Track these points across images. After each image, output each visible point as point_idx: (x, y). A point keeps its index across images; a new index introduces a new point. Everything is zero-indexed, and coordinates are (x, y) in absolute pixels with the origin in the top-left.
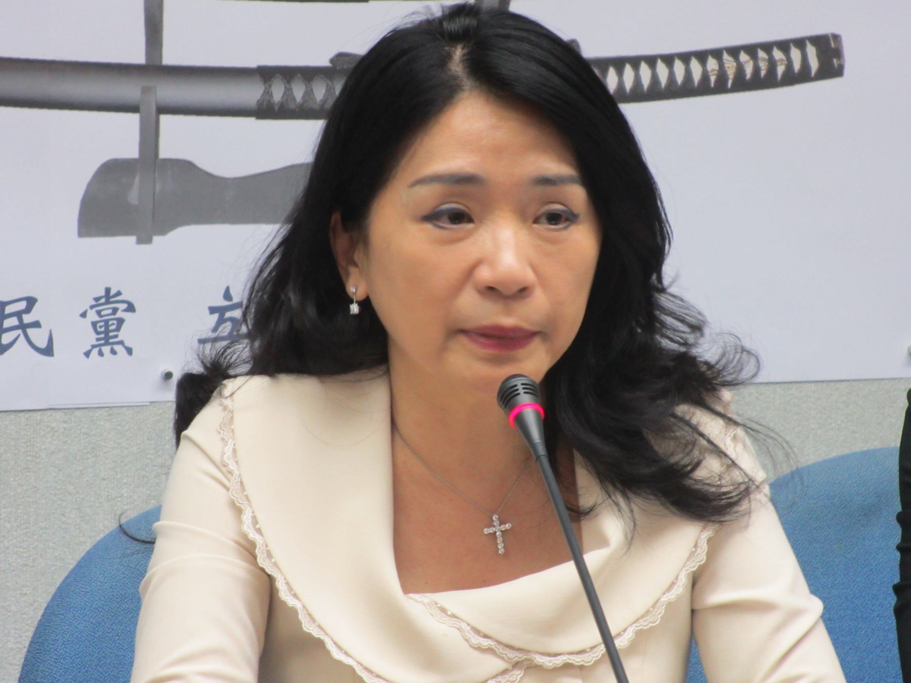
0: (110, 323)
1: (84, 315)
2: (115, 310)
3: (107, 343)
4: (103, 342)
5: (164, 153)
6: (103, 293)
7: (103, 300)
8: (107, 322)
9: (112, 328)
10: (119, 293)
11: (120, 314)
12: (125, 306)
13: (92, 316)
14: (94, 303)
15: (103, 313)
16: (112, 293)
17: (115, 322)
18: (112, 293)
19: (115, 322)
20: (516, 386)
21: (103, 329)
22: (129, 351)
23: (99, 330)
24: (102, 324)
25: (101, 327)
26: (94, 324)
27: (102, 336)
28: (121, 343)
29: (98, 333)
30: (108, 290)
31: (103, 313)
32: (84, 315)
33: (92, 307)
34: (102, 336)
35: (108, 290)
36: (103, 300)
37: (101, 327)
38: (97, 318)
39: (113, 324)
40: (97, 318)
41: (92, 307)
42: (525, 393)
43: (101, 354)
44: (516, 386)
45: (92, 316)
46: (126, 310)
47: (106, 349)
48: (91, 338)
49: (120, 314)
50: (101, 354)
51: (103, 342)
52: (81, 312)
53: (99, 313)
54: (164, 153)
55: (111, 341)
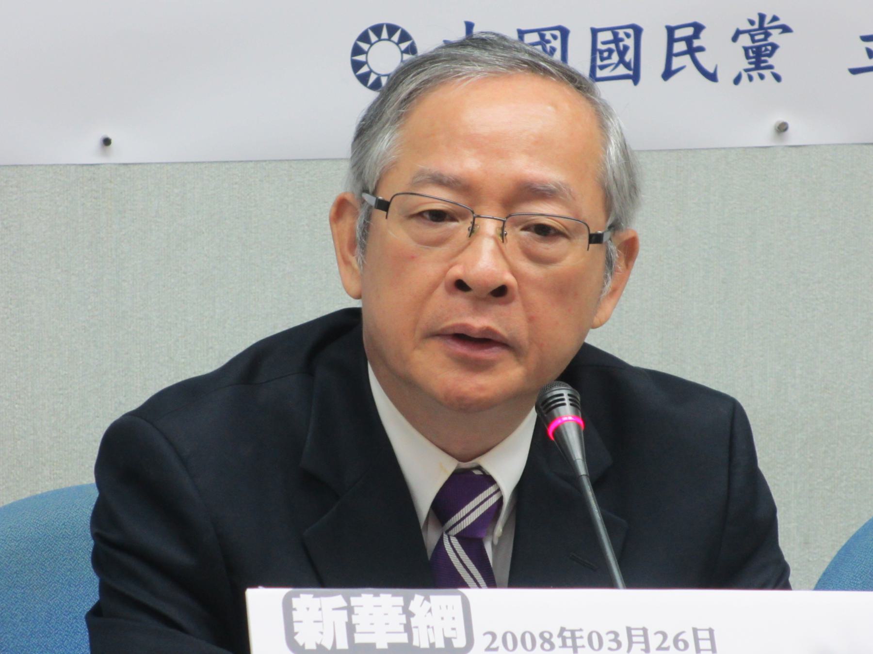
3: (758, 67)
4: (753, 66)
8: (759, 48)
13: (745, 40)
22: (777, 78)
26: (746, 49)
27: (753, 60)
28: (770, 67)
29: (748, 57)
34: (753, 60)
43: (751, 78)
47: (755, 74)
48: (745, 64)
50: (751, 78)
51: (753, 66)
55: (763, 65)
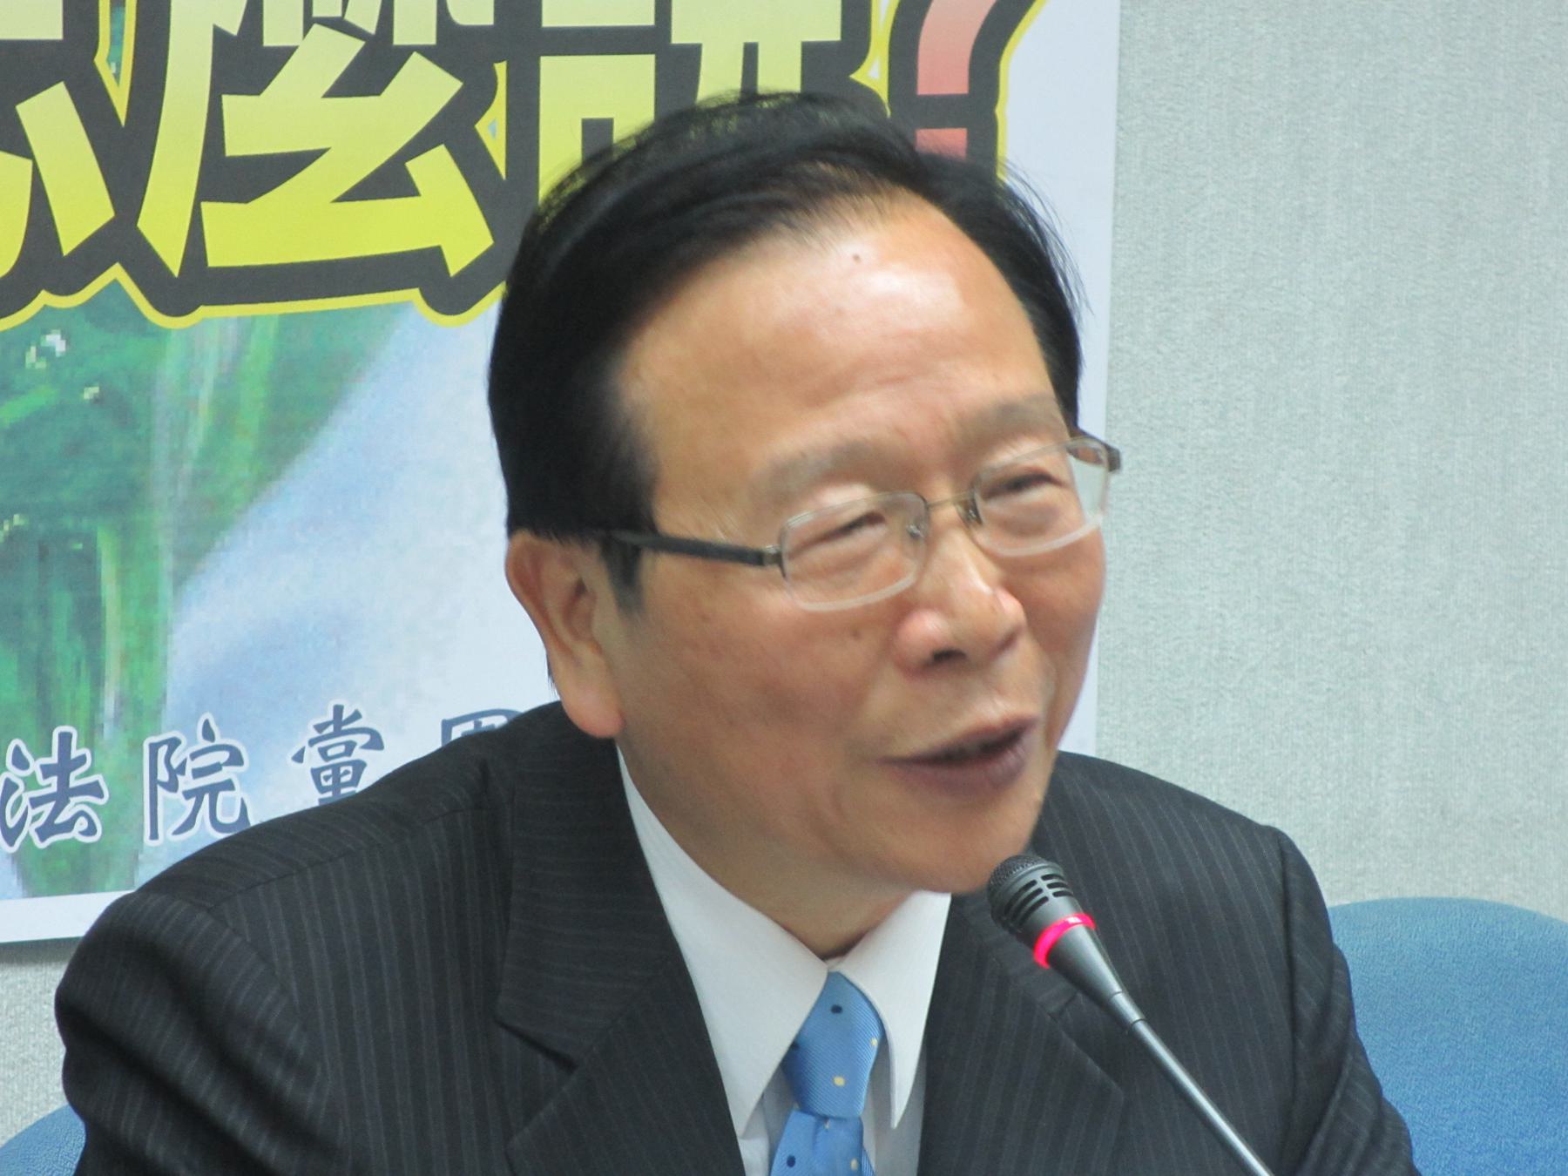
0: (342, 770)
1: (299, 758)
2: (350, 747)
5: (546, 62)
6: (330, 716)
7: (330, 729)
8: (336, 768)
9: (345, 779)
10: (356, 716)
11: (358, 754)
12: (366, 738)
13: (313, 759)
14: (315, 734)
15: (330, 753)
16: (346, 715)
17: (350, 769)
18: (346, 715)
19: (350, 769)
20: (1033, 883)
21: (330, 782)
23: (324, 783)
24: (329, 772)
25: (327, 778)
26: (316, 773)
29: (322, 789)
30: (338, 710)
31: (330, 753)
32: (299, 758)
33: (312, 742)
35: (338, 710)
36: (330, 729)
37: (327, 778)
38: (321, 763)
39: (346, 773)
40: (321, 763)
41: (312, 742)
42: (1056, 894)
44: (1033, 883)
45: (313, 759)
46: (366, 747)
49: (358, 754)
52: (295, 751)
53: (323, 752)
54: (546, 62)
